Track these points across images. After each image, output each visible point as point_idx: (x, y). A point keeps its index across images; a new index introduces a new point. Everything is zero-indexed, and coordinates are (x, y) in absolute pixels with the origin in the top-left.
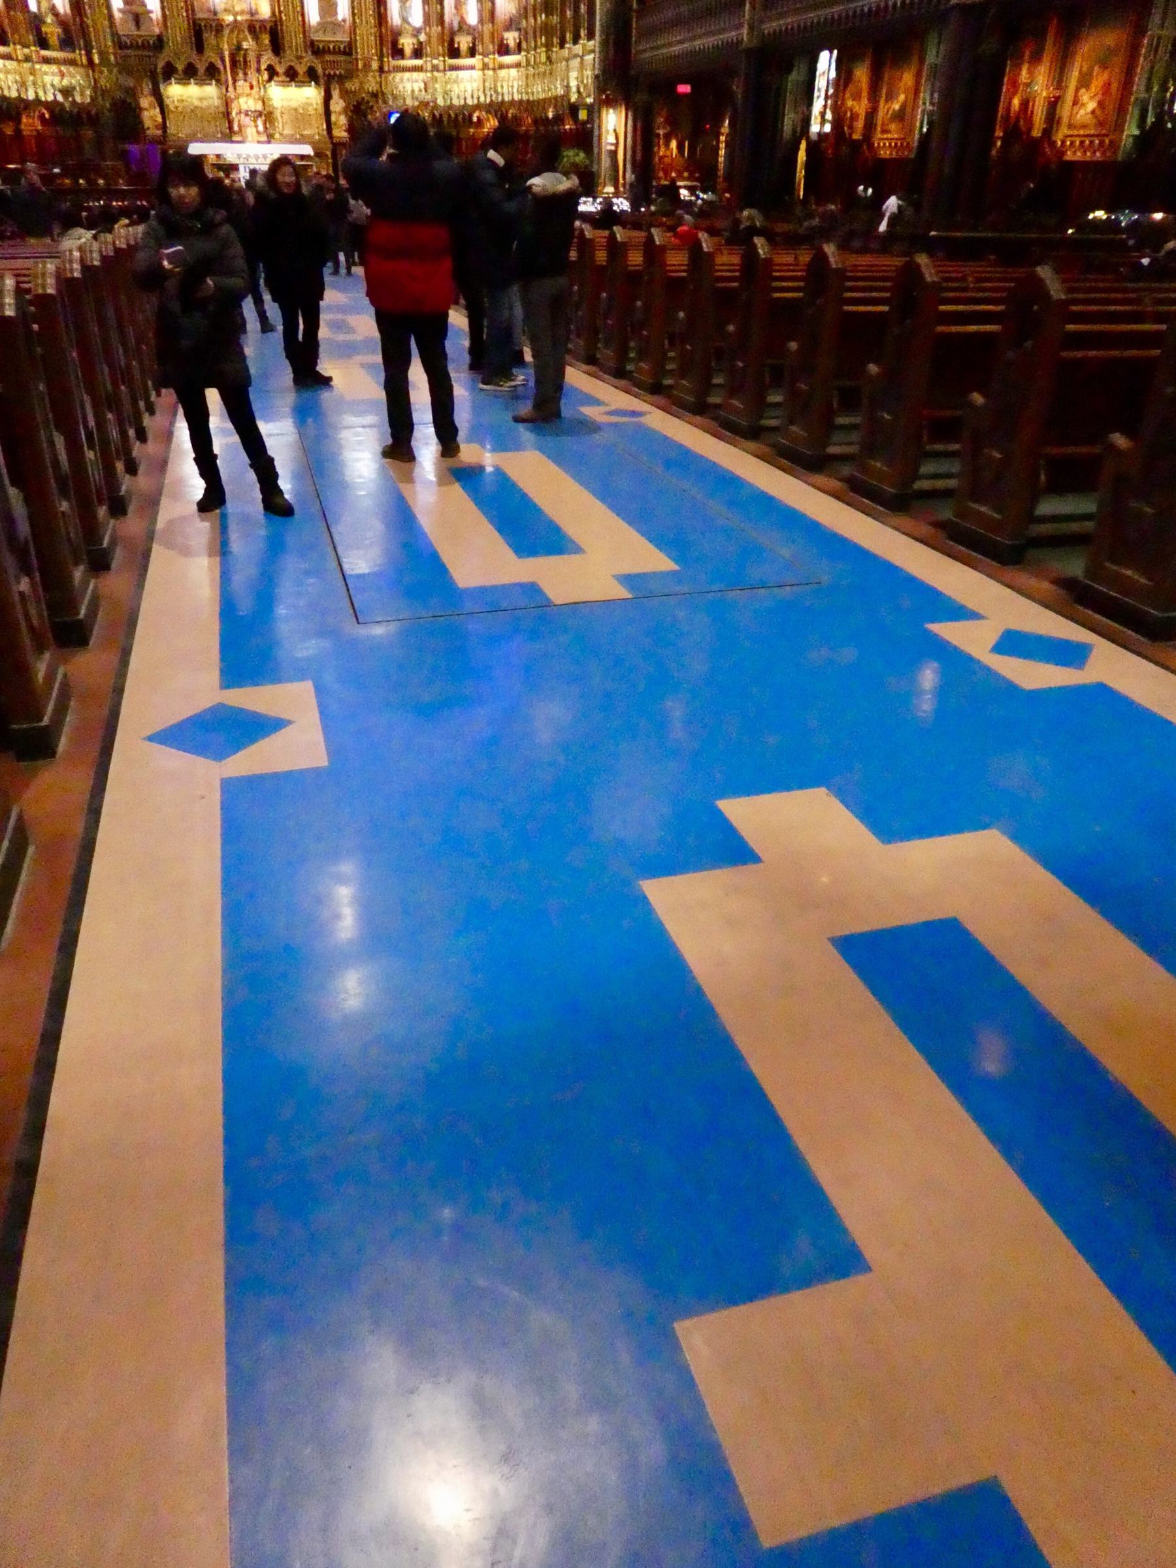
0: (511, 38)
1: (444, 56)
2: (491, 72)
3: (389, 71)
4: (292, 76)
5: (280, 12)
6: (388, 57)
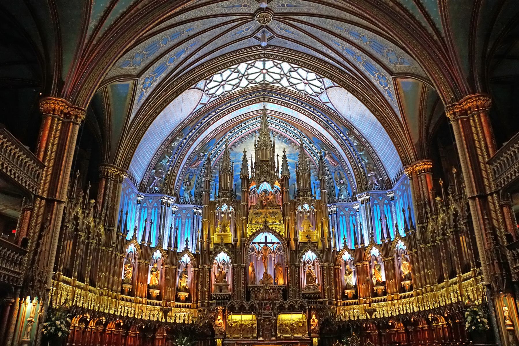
2: (396, 301)
3: (340, 306)
4: (292, 310)
5: (288, 282)
6: (340, 299)
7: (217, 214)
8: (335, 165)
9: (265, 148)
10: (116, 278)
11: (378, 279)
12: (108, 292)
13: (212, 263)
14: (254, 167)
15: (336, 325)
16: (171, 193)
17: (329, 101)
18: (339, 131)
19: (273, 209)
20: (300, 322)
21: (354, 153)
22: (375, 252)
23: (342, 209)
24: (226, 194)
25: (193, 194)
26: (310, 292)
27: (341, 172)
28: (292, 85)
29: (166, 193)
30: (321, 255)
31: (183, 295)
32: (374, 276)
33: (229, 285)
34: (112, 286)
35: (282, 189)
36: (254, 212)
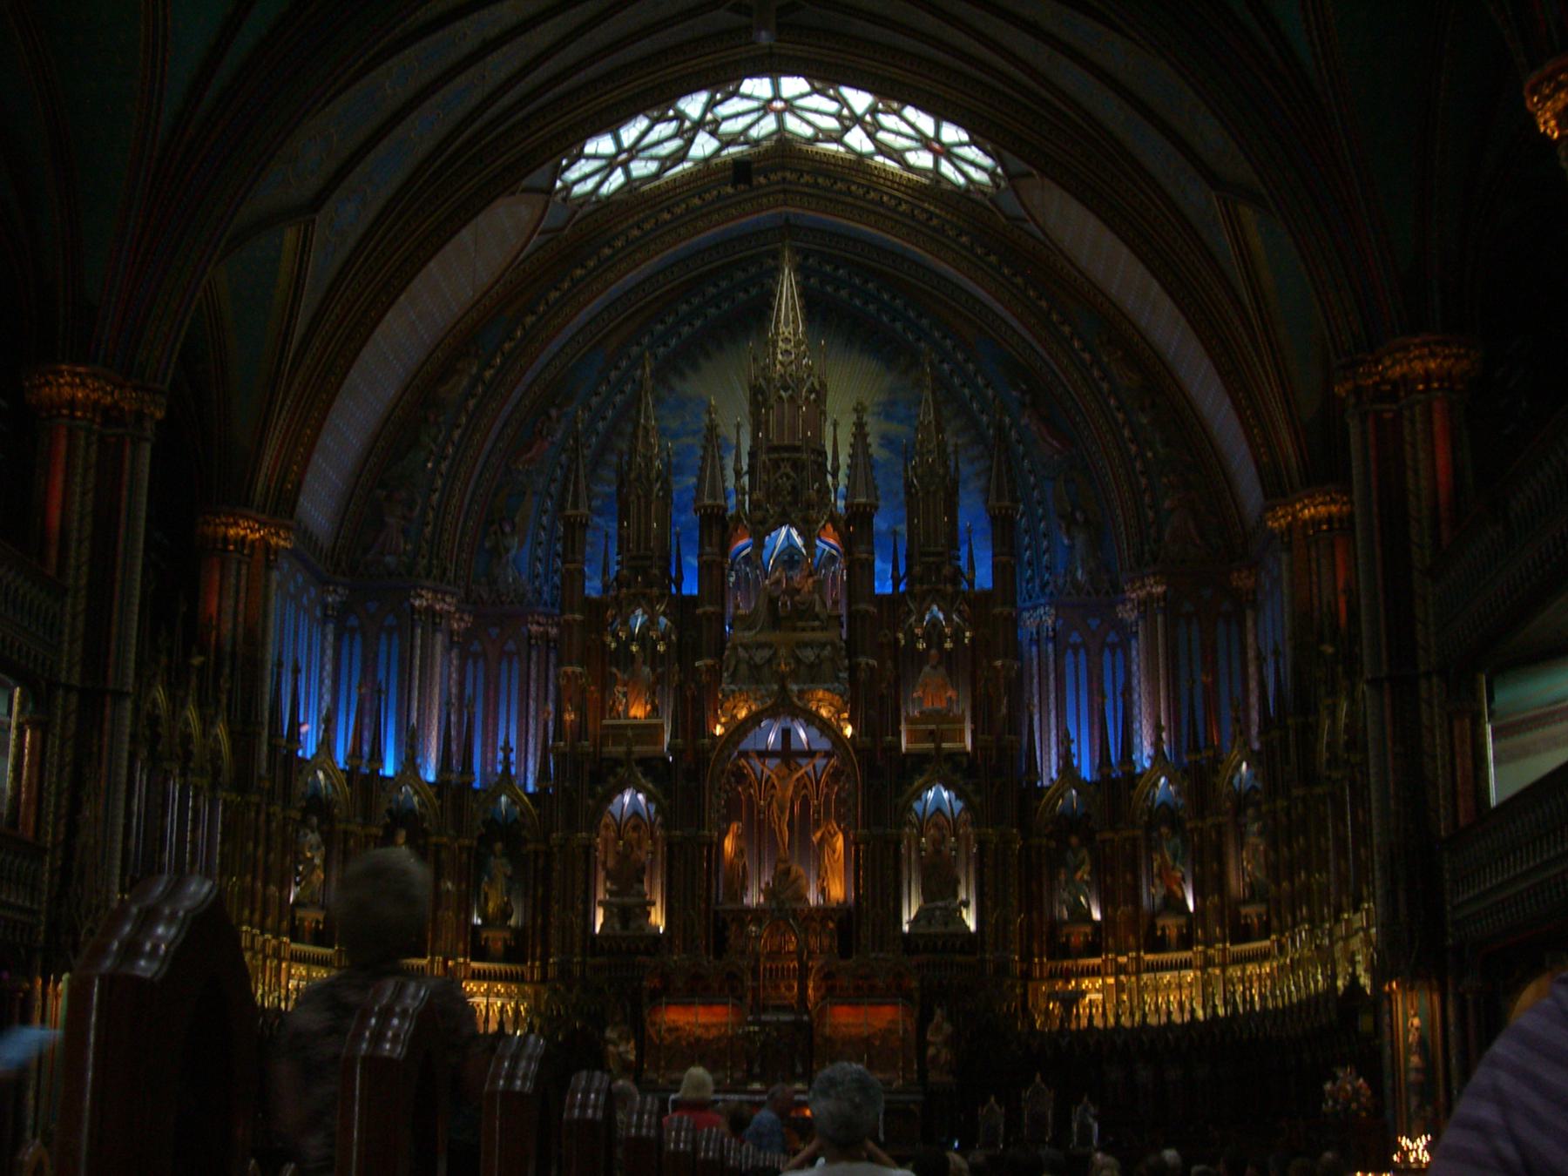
0: (1252, 912)
1: (1138, 951)
3: (1042, 978)
4: (864, 993)
6: (1041, 957)
7: (613, 645)
10: (273, 889)
12: (253, 936)
13: (593, 827)
14: (745, 468)
16: (445, 571)
18: (1066, 329)
19: (813, 629)
26: (932, 930)
29: (428, 575)
31: (496, 939)
32: (1157, 881)
33: (654, 904)
34: (264, 916)
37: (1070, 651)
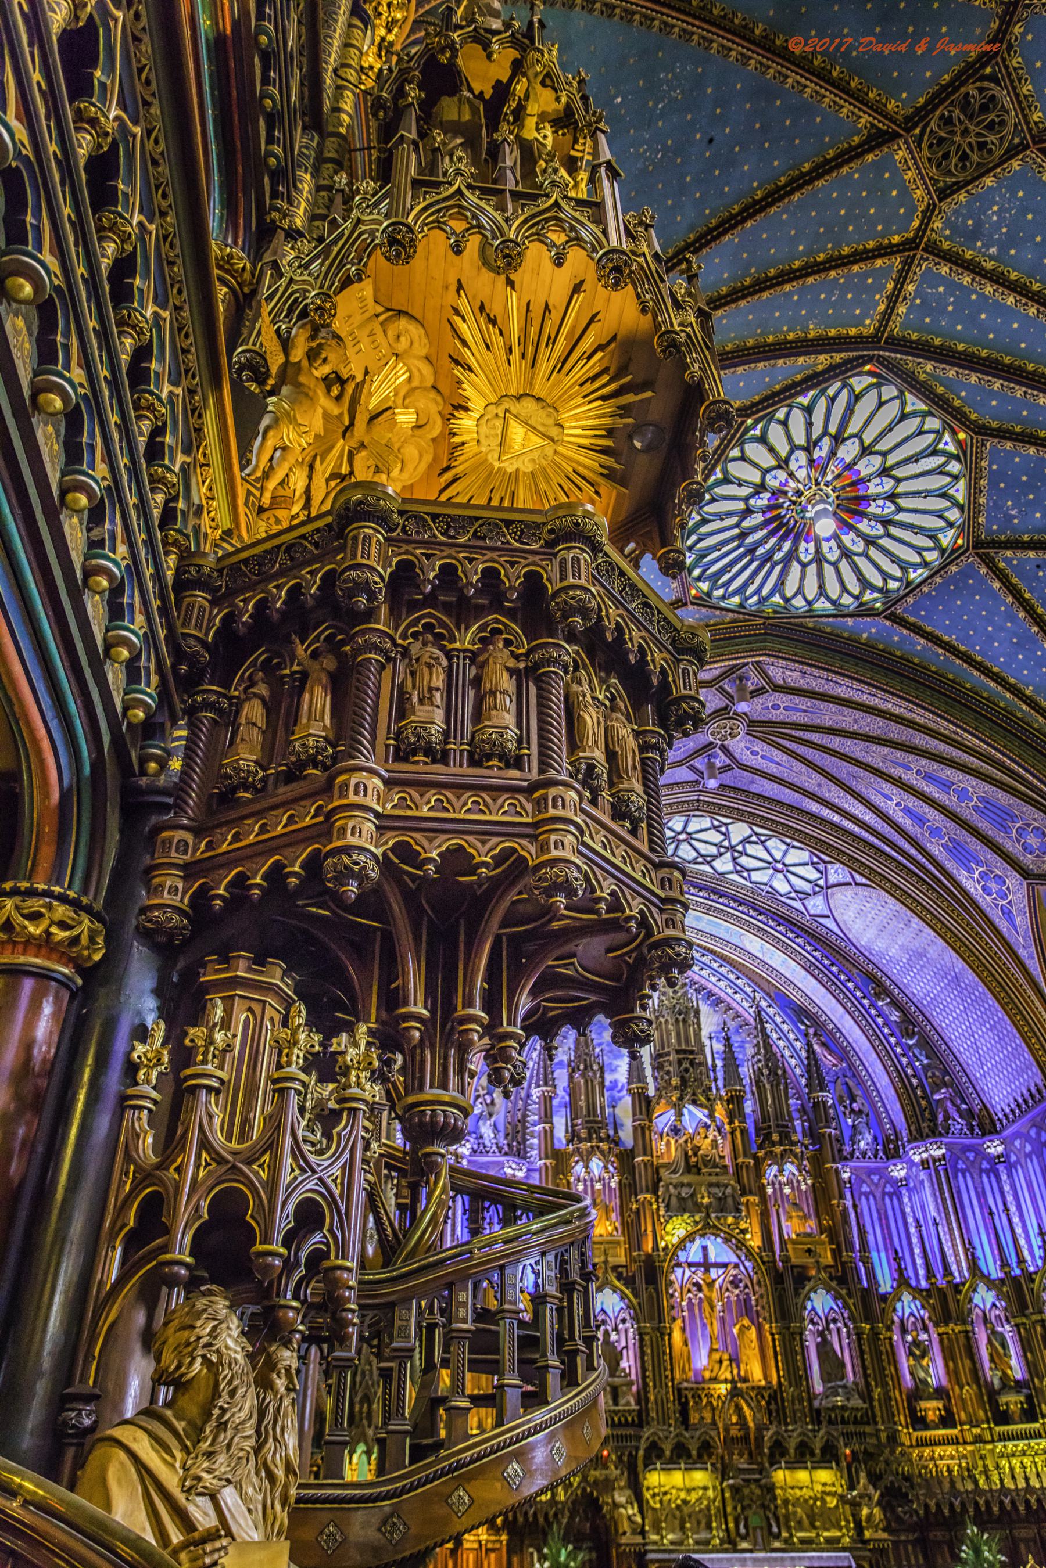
1: (988, 1422)
3: (911, 1446)
5: (779, 1377)
8: (834, 1065)
9: (681, 1018)
11: (1004, 1373)
15: (919, 1505)
17: (828, 913)
18: (850, 985)
20: (829, 1494)
21: (893, 1040)
22: (984, 1298)
23: (864, 1177)
24: (598, 1133)
25: (501, 1127)
27: (851, 1083)
28: (740, 870)
30: (851, 1302)
35: (731, 1123)
36: (674, 1182)
37: (863, 1198)
